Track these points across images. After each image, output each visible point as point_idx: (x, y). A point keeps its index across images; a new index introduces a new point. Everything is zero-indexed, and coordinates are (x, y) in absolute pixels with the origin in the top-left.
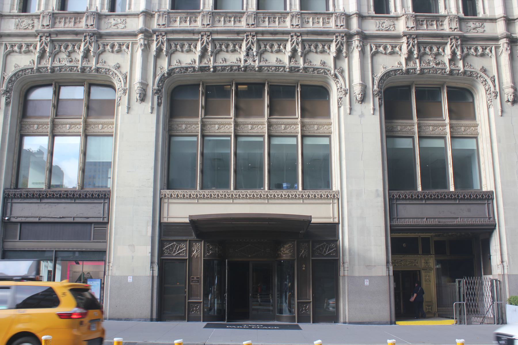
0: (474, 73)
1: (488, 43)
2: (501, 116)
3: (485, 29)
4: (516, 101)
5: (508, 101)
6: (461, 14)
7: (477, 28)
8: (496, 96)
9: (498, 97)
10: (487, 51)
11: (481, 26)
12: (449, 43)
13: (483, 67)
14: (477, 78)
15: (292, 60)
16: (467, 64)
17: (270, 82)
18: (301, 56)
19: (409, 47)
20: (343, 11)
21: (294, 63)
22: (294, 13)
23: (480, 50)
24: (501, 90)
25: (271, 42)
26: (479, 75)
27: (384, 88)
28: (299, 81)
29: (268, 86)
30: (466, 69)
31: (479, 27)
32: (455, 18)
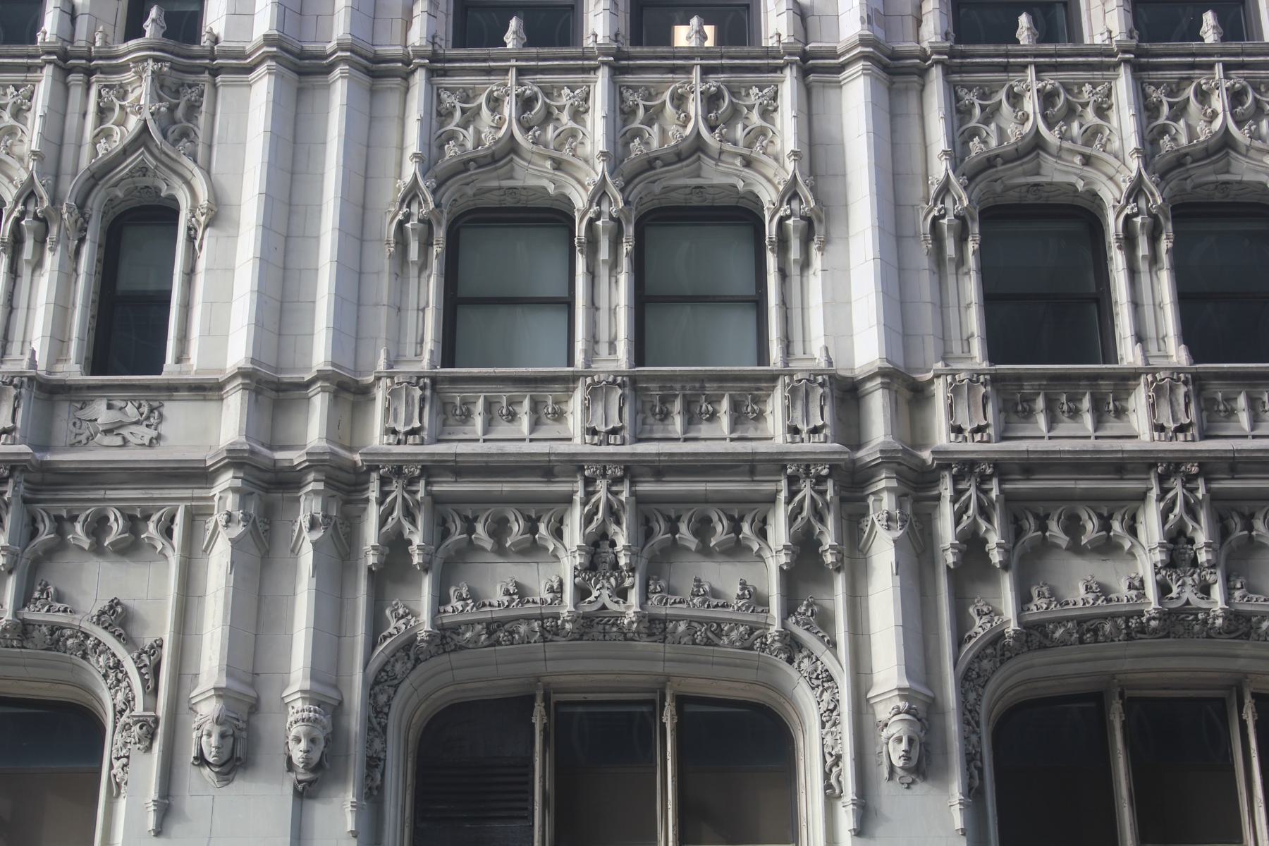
0: (68, 632)
1: (157, 494)
2: (159, 832)
3: (163, 429)
4: (239, 759)
5: (201, 760)
6: (72, 370)
7: (122, 425)
8: (151, 736)
9: (157, 746)
10: (151, 529)
11: (148, 418)
12: (1154, 493)
13: (114, 604)
14: (84, 656)
15: (652, 587)
16: (42, 592)
17: (557, 691)
18: (426, 568)
19: (1171, 516)
20: (823, 365)
21: (703, 603)
22: (602, 377)
23: (116, 527)
24: (184, 706)
25: (493, 508)
26: (90, 643)
27: (990, 712)
28: (668, 677)
29: (547, 708)
30: (27, 616)
31: (137, 423)
32: (11, 383)
